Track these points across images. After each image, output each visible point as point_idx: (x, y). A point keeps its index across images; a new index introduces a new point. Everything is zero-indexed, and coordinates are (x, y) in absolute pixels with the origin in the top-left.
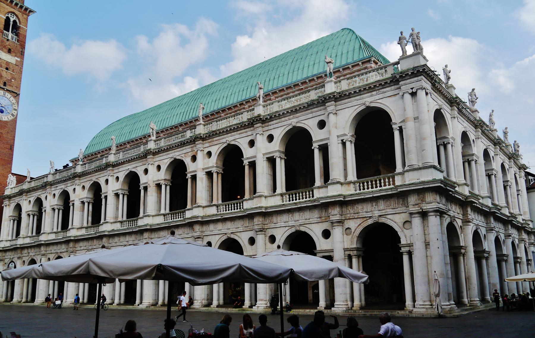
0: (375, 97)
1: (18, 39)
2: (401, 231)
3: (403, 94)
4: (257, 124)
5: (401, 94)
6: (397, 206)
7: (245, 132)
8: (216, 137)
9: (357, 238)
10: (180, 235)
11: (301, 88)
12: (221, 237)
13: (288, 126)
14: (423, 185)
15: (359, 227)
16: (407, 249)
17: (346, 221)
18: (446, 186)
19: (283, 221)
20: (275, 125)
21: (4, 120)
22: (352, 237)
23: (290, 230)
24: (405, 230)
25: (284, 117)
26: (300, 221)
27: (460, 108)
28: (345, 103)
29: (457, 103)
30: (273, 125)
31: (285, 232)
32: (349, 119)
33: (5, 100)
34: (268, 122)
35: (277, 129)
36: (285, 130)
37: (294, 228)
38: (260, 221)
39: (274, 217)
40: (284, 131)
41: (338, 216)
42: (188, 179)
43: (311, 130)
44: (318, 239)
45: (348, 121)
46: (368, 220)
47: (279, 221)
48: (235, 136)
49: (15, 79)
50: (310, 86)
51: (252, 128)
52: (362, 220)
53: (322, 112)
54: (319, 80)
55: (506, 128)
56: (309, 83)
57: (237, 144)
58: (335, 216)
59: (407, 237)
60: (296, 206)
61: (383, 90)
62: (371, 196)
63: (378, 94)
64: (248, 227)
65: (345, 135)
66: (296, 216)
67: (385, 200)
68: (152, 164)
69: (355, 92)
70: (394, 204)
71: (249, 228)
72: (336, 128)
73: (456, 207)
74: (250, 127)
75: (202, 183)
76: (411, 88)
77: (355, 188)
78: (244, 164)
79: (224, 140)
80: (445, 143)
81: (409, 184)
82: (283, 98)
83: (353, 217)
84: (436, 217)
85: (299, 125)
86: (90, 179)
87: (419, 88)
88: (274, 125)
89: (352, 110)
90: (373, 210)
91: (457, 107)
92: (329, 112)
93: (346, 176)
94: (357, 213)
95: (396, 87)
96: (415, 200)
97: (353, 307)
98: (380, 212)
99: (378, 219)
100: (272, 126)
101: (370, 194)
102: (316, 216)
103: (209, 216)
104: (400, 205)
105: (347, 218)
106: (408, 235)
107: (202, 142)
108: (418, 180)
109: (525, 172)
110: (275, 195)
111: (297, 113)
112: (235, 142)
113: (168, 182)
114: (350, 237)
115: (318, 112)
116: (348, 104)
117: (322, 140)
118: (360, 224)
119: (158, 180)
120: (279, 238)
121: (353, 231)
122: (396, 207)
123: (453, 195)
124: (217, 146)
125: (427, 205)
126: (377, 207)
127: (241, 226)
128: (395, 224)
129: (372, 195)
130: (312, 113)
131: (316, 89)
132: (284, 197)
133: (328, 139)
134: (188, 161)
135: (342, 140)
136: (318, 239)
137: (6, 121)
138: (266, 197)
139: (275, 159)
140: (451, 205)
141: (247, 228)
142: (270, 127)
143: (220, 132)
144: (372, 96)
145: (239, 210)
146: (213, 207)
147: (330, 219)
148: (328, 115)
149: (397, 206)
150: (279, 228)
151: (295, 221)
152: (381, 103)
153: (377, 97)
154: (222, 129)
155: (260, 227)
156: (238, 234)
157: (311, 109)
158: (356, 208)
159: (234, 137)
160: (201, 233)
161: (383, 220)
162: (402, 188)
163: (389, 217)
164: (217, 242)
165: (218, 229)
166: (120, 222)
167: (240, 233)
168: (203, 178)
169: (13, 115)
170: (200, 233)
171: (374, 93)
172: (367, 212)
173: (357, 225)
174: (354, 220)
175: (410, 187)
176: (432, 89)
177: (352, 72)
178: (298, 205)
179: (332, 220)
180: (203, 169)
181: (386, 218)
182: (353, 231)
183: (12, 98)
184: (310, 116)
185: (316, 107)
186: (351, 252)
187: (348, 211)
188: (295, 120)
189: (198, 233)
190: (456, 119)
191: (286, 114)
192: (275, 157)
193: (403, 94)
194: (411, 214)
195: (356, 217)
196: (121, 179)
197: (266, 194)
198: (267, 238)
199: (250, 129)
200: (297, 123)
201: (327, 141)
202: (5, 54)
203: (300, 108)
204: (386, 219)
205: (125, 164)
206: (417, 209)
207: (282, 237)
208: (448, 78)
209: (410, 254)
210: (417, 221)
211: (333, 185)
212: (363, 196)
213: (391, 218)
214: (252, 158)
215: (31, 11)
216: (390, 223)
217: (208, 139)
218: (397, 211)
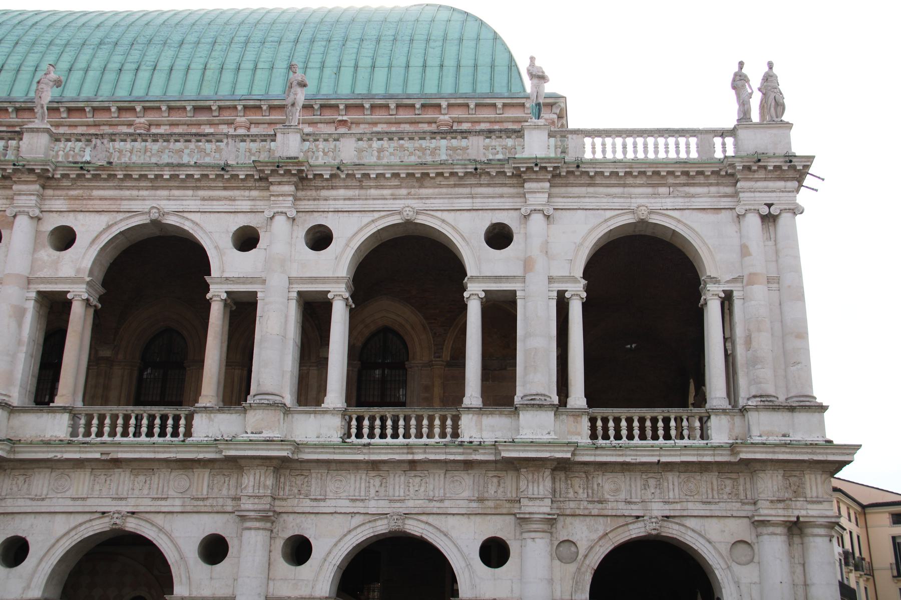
0: (664, 200)
2: (724, 566)
4: (280, 183)
5: (740, 210)
6: (716, 496)
7: (226, 199)
8: (103, 188)
11: (340, 118)
12: (81, 525)
13: (388, 216)
14: (811, 453)
15: (600, 543)
17: (561, 518)
19: (345, 494)
20: (342, 202)
22: (579, 569)
23: (368, 526)
24: (734, 565)
25: (377, 187)
26: (410, 503)
28: (579, 197)
30: (335, 200)
31: (350, 531)
32: (585, 239)
34: (317, 188)
35: (346, 214)
36: (377, 224)
37: (385, 521)
38: (265, 487)
39: (313, 481)
40: (373, 226)
41: (548, 502)
43: (463, 243)
44: (468, 565)
45: (581, 244)
46: (631, 527)
47: (330, 495)
48: (184, 203)
50: (370, 121)
52: (610, 524)
53: (508, 203)
54: (401, 111)
56: (369, 112)
57: (187, 226)
58: (537, 502)
59: (742, 587)
60: (410, 457)
61: (687, 189)
63: (674, 197)
64: (203, 499)
66: (398, 484)
67: (683, 476)
70: (710, 491)
71: (208, 503)
74: (250, 189)
76: (765, 204)
77: (593, 428)
78: (208, 296)
79: (136, 206)
81: (776, 445)
82: (375, 129)
83: (586, 512)
85: (422, 220)
87: (787, 207)
88: (337, 202)
89: (594, 219)
90: (645, 498)
92: (533, 208)
94: (600, 502)
95: (729, 190)
96: (775, 488)
100: (331, 202)
101: (653, 455)
102: (466, 494)
103: (323, 446)
104: (725, 497)
105: (568, 512)
107: (41, 190)
108: (784, 436)
111: (420, 187)
112: (182, 221)
114: (572, 567)
115: (490, 200)
116: (587, 200)
117: (498, 279)
120: (327, 549)
121: (582, 552)
122: (713, 498)
125: (809, 506)
126: (658, 491)
127: (176, 495)
128: (707, 544)
130: (473, 198)
131: (489, 133)
136: (468, 565)
142: (322, 205)
144: (655, 195)
145: (437, 439)
146: (58, 416)
147: (520, 508)
149: (716, 496)
151: (391, 501)
152: (679, 221)
154: (142, 166)
155: (264, 504)
156: (159, 519)
157: (471, 186)
158: (595, 486)
159: (179, 202)
161: (672, 531)
162: (755, 452)
164: (58, 541)
165: (68, 494)
167: (169, 516)
171: (663, 190)
172: (630, 503)
173: (595, 536)
174: (588, 519)
175: (774, 453)
177: (497, 120)
178: (417, 453)
180: (29, 281)
181: (683, 525)
182: (582, 552)
184: (466, 203)
185: (488, 185)
187: (571, 491)
188: (417, 204)
191: (387, 179)
192: (69, 296)
193: (273, 216)
194: (759, 524)
195: (595, 512)
198: (279, 544)
199: (247, 193)
200: (417, 213)
201: (514, 285)
204: (683, 529)
206: (781, 512)
207: (336, 545)
211: (536, 413)
212: (630, 455)
213: (697, 528)
214: (244, 283)
216: (694, 541)
217: (69, 188)
218: (716, 510)
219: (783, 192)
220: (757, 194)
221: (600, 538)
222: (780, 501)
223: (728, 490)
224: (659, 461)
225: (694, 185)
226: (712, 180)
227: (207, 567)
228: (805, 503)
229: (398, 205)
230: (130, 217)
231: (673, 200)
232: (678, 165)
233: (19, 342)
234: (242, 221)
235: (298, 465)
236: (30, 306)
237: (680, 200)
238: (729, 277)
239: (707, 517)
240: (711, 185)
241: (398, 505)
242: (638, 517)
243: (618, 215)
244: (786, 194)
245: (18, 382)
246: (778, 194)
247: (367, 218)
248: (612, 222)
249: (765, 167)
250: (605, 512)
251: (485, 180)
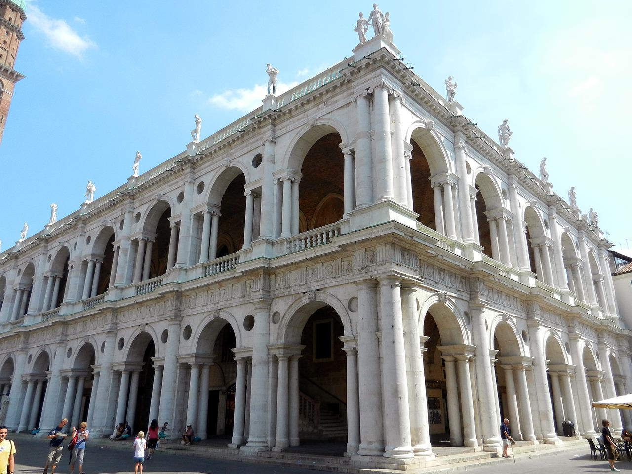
3: (356, 100)
4: (187, 169)
9: (288, 329)
10: (94, 330)
13: (220, 169)
15: (289, 310)
16: (352, 344)
18: (412, 237)
22: (280, 326)
23: (208, 317)
24: (350, 312)
26: (221, 304)
27: (473, 136)
29: (463, 127)
31: (202, 321)
32: (289, 148)
41: (261, 292)
42: (114, 252)
45: (287, 150)
46: (302, 299)
51: (183, 177)
55: (573, 188)
58: (258, 293)
59: (353, 325)
60: (214, 281)
62: (303, 258)
63: (326, 107)
65: (282, 171)
68: (81, 235)
69: (296, 108)
70: (337, 271)
72: (274, 163)
73: (453, 279)
75: (126, 255)
77: (290, 248)
79: (153, 197)
80: (442, 183)
83: (283, 295)
84: (392, 287)
86: (25, 260)
89: (292, 134)
91: (463, 133)
93: (280, 231)
97: (274, 446)
98: (317, 284)
99: (315, 296)
104: (345, 272)
105: (276, 297)
106: (354, 322)
107: (132, 201)
109: (609, 251)
110: (197, 267)
113: (98, 258)
114: (277, 326)
116: (290, 126)
117: (256, 182)
118: (292, 305)
119: (86, 256)
121: (281, 317)
123: (440, 257)
124: (147, 205)
125: (379, 268)
129: (305, 257)
132: (207, 269)
133: (260, 180)
134: (116, 228)
135: (279, 179)
138: (186, 270)
139: (204, 215)
140: (440, 275)
141: (162, 316)
143: (149, 185)
148: (264, 145)
150: (197, 315)
153: (325, 110)
156: (152, 325)
160: (115, 326)
163: (331, 291)
164: (129, 339)
165: (133, 319)
166: (43, 314)
168: (128, 249)
170: (112, 325)
171: (321, 105)
172: (300, 285)
174: (285, 298)
176: (404, 92)
179: (252, 299)
182: (281, 317)
184: (246, 150)
186: (278, 351)
188: (229, 158)
189: (109, 325)
190: (463, 150)
195: (287, 294)
196: (53, 258)
197: (188, 266)
198: (183, 330)
203: (234, 141)
205: (58, 238)
207: (198, 328)
208: (453, 94)
209: (356, 353)
210: (363, 296)
215: (17, 76)
218: (340, 280)
219: (374, 77)
220: (362, 85)
221: (289, 308)
222: (363, 268)
223: (346, 267)
225: (336, 95)
226: (344, 88)
227: (164, 344)
228: (377, 266)
229: (222, 162)
230: (153, 202)
231: (327, 108)
232: (323, 88)
233: (126, 262)
234: (179, 191)
235: (186, 293)
236: (129, 247)
237: (330, 107)
238: (350, 142)
239: (338, 286)
240: (344, 91)
241: (216, 305)
242: (305, 293)
243: (301, 130)
244: (376, 78)
245: (125, 278)
246: (373, 80)
247: (216, 171)
248: (300, 133)
249: (361, 67)
250: (291, 293)
251: (251, 135)
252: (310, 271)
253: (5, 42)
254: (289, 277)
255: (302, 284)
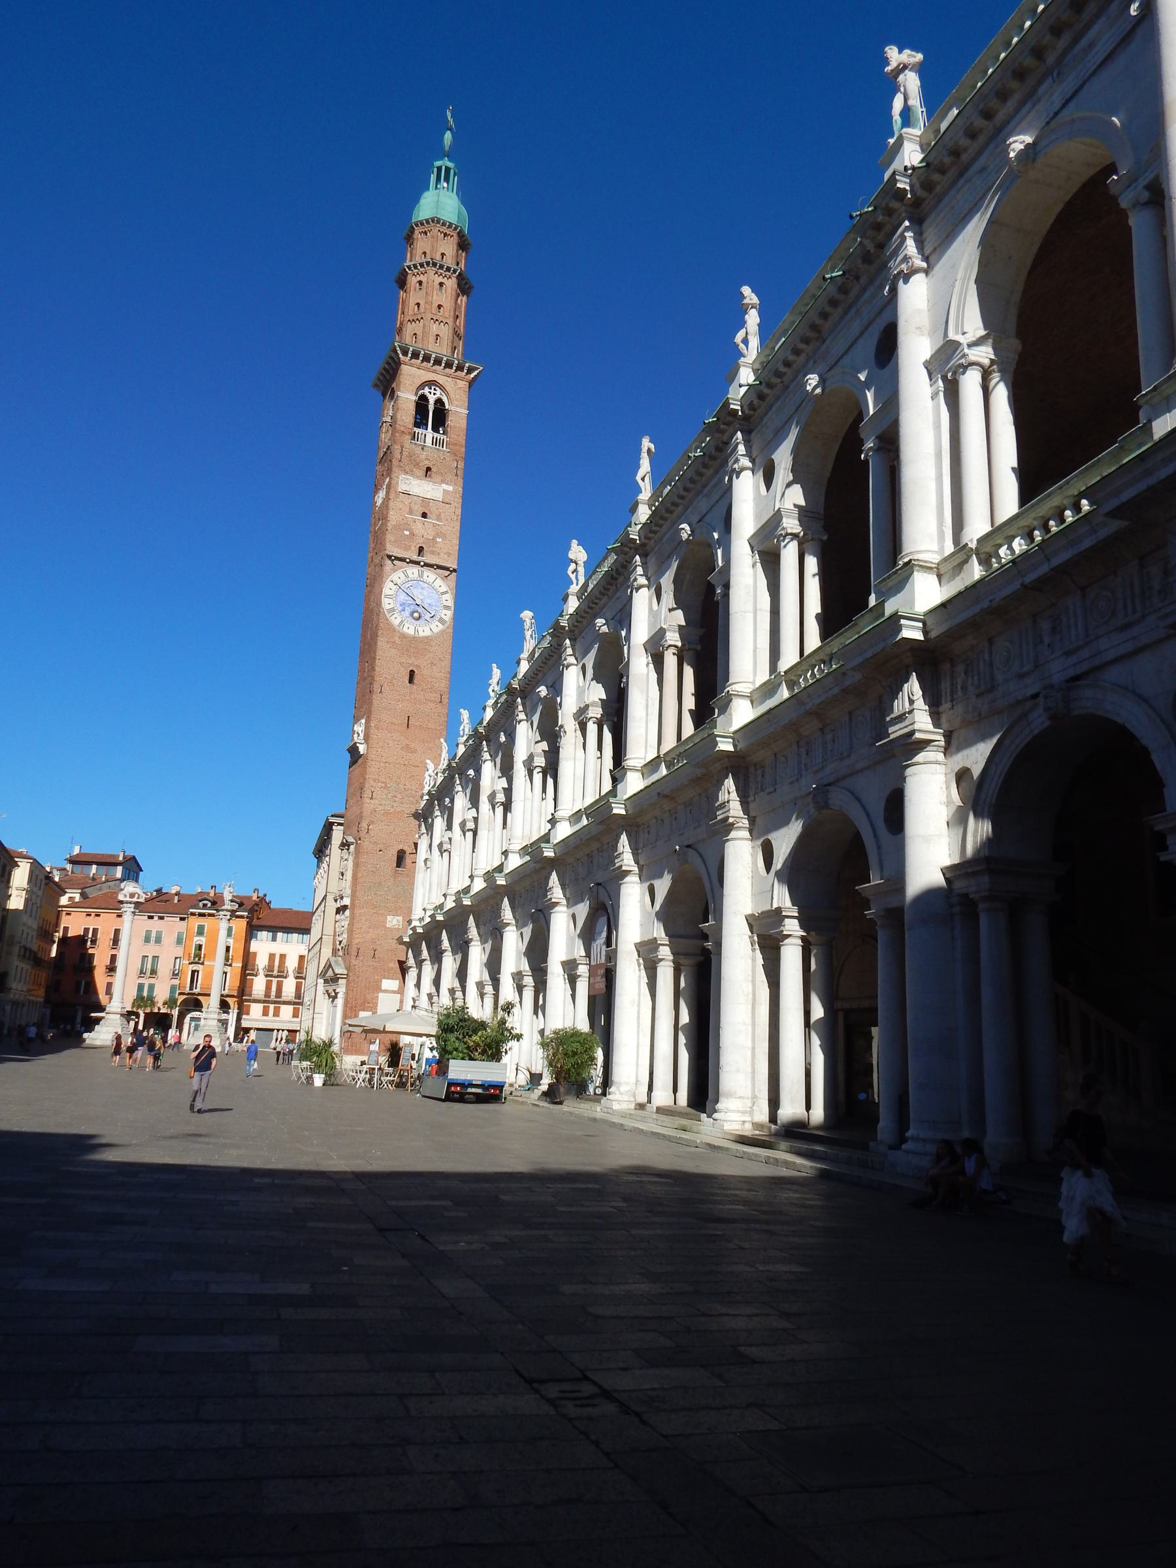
1: (447, 441)
21: (421, 634)
33: (422, 588)
49: (443, 536)
61: (1084, 42)
137: (427, 638)
169: (441, 621)
172: (1021, 676)
183: (439, 582)
202: (419, 481)
224: (1022, 585)
252: (1045, 625)
253: (440, 307)
254: (987, 657)
255: (1025, 669)
